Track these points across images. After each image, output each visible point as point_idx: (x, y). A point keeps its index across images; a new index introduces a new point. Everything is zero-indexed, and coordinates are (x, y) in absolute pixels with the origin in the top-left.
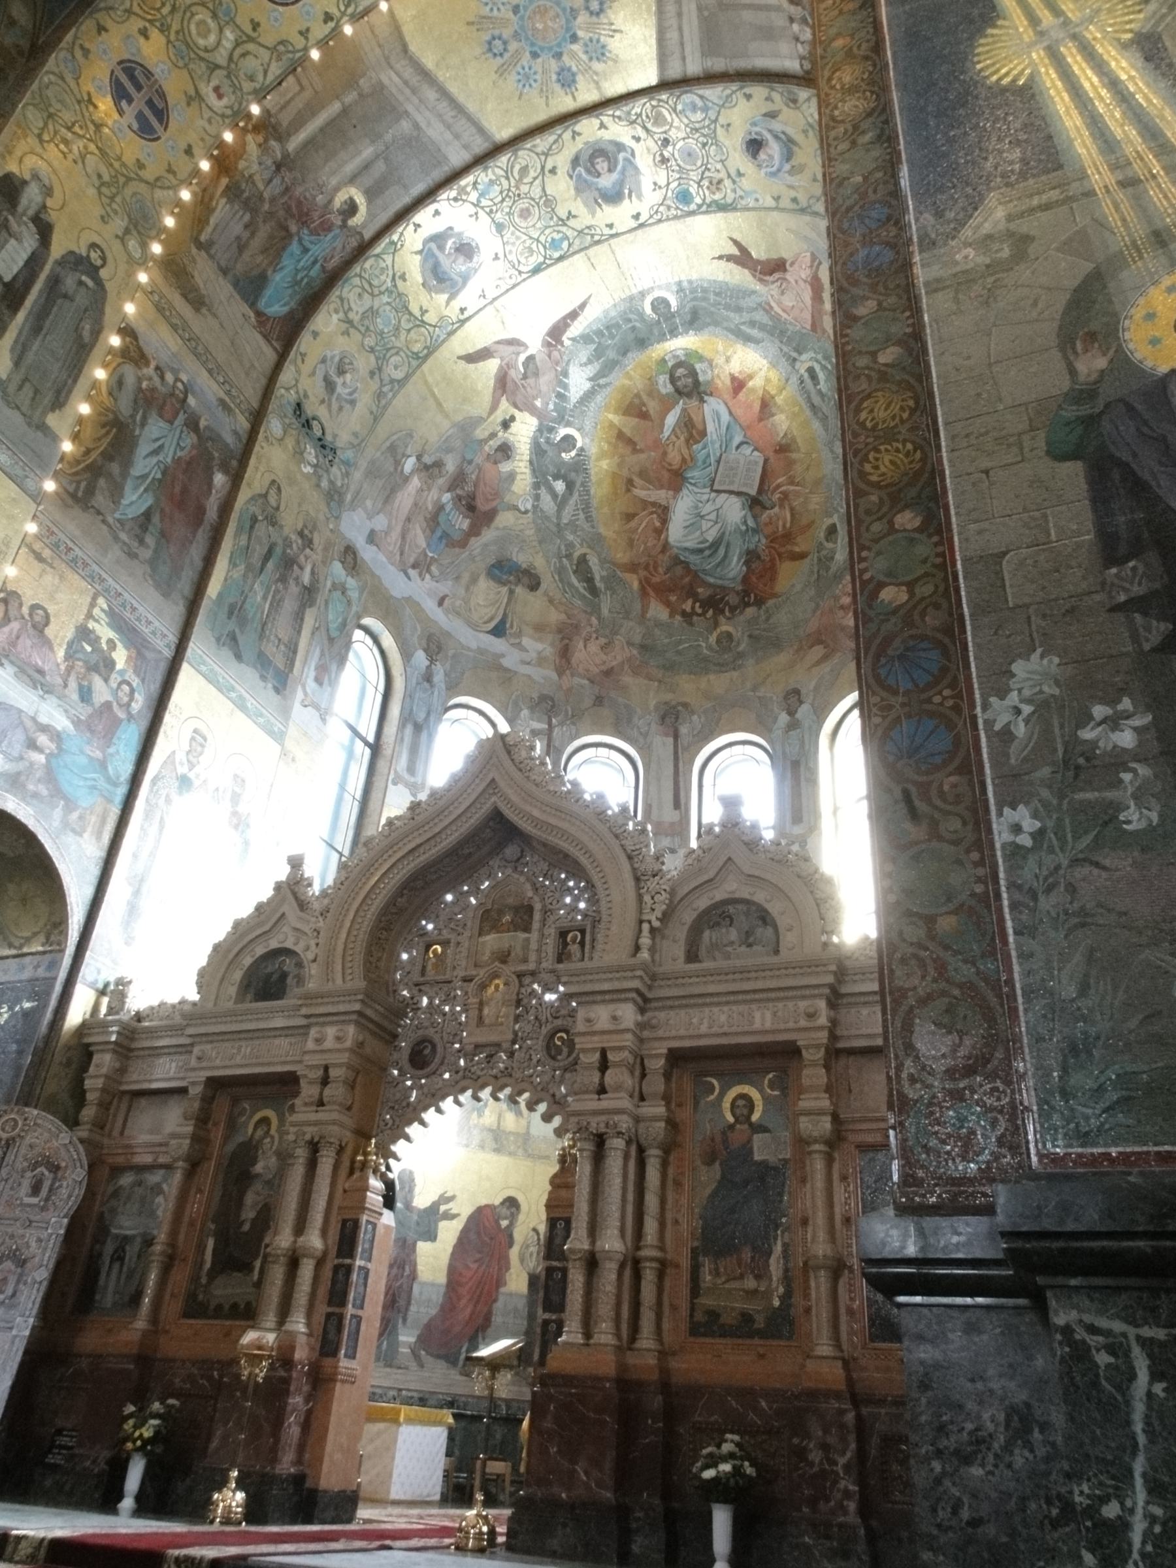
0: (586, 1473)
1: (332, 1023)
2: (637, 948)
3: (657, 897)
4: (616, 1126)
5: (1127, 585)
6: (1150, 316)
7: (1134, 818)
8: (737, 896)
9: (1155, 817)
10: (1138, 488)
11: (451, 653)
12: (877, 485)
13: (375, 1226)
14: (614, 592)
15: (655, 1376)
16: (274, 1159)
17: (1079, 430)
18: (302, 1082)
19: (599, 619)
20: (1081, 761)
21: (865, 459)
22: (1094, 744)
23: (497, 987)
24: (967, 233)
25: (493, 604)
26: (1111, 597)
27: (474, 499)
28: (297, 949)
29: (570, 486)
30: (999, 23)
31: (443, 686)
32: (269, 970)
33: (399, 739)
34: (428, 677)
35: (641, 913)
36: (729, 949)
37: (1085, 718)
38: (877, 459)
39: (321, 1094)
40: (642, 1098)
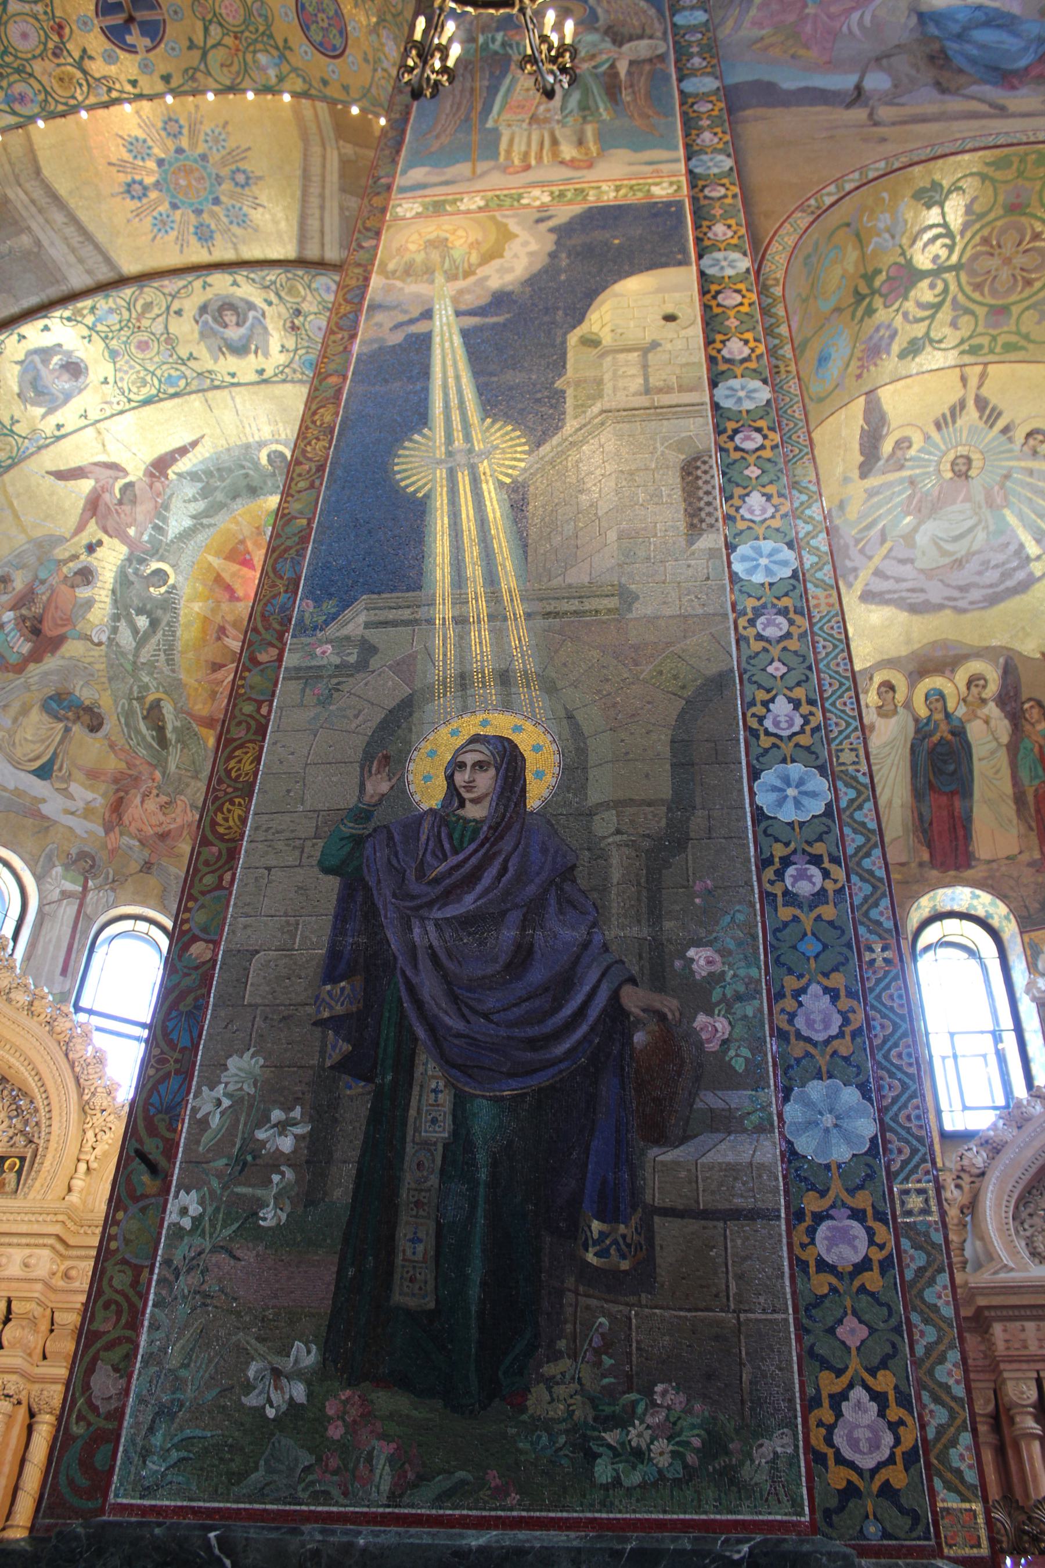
5: (333, 1003)
6: (432, 753)
7: (270, 1217)
9: (284, 1217)
10: (371, 914)
12: (221, 837)
14: (185, 745)
17: (347, 849)
19: (164, 774)
20: (249, 1158)
21: (220, 809)
22: (263, 1143)
24: (331, 631)
25: (43, 741)
26: (318, 1012)
27: (40, 622)
29: (154, 624)
30: (426, 431)
37: (263, 1120)
38: (229, 811)
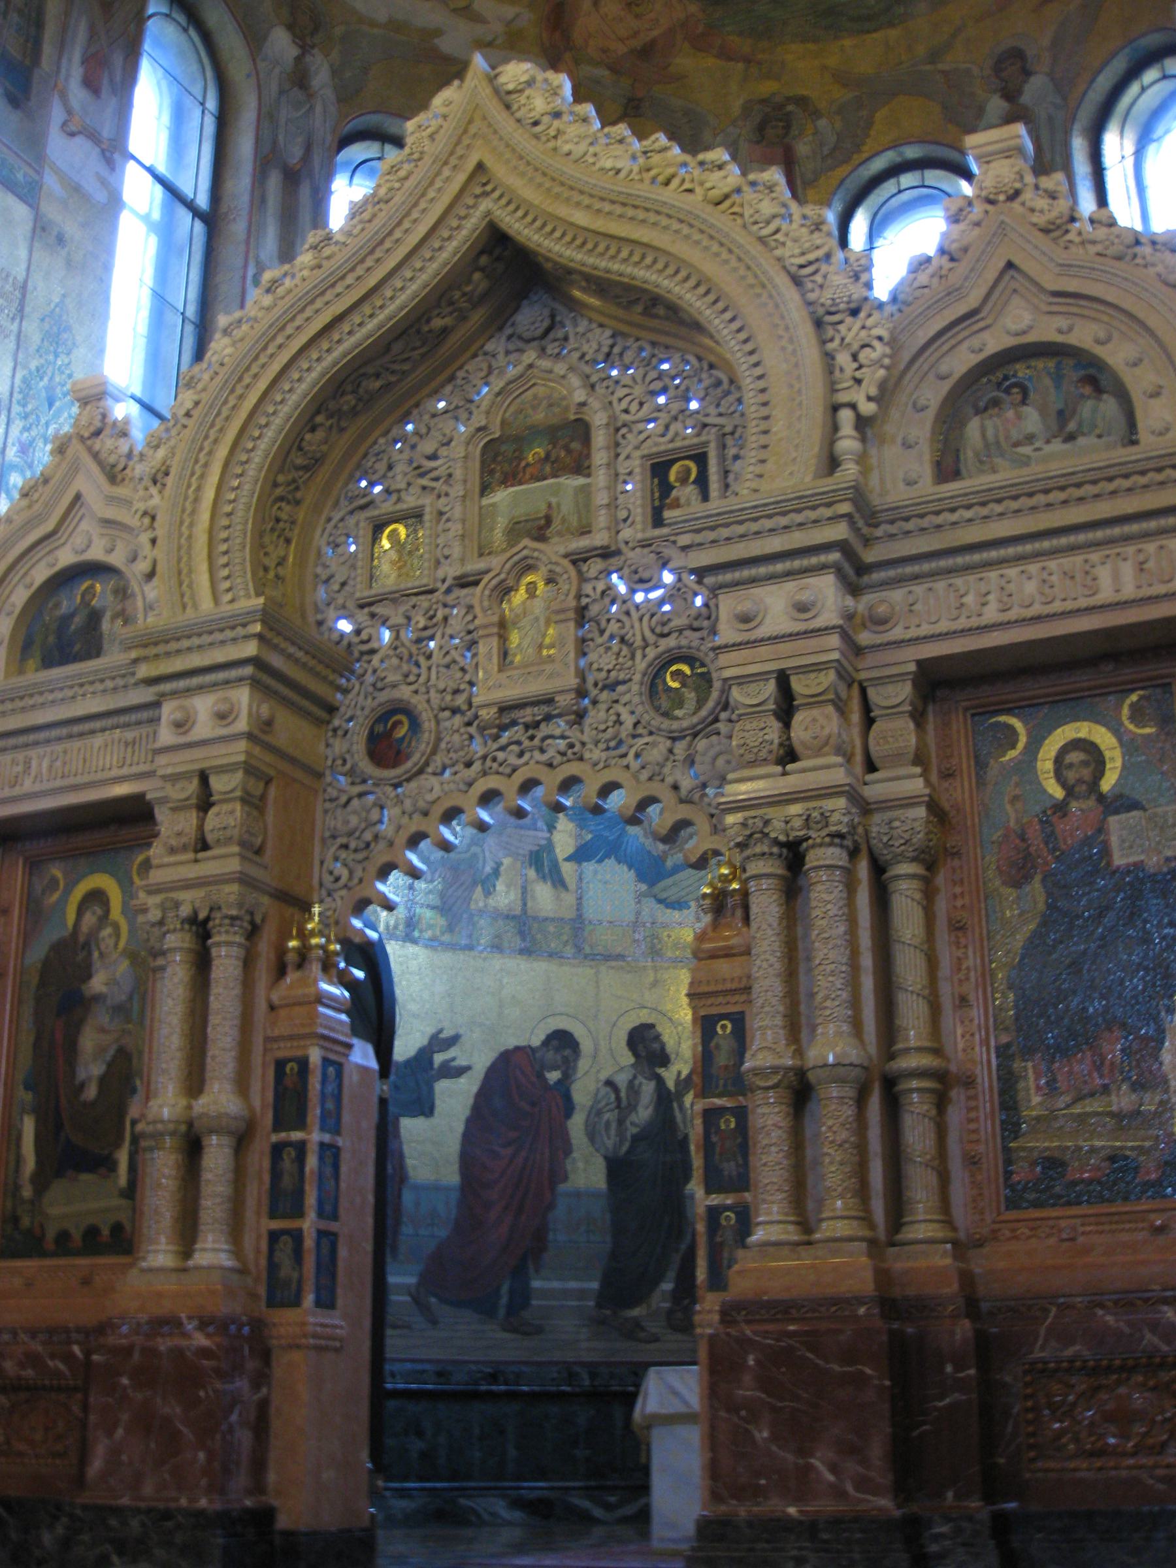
0: (834, 1469)
1: (201, 688)
2: (832, 463)
3: (864, 355)
4: (825, 818)
8: (1031, 338)
11: (339, 31)
13: (339, 1067)
15: (952, 1288)
16: (124, 966)
18: (161, 814)
23: (531, 589)
28: (117, 559)
31: (329, 93)
32: (65, 607)
33: (259, 200)
34: (300, 78)
35: (833, 389)
36: (1026, 450)
39: (201, 828)
40: (871, 767)
